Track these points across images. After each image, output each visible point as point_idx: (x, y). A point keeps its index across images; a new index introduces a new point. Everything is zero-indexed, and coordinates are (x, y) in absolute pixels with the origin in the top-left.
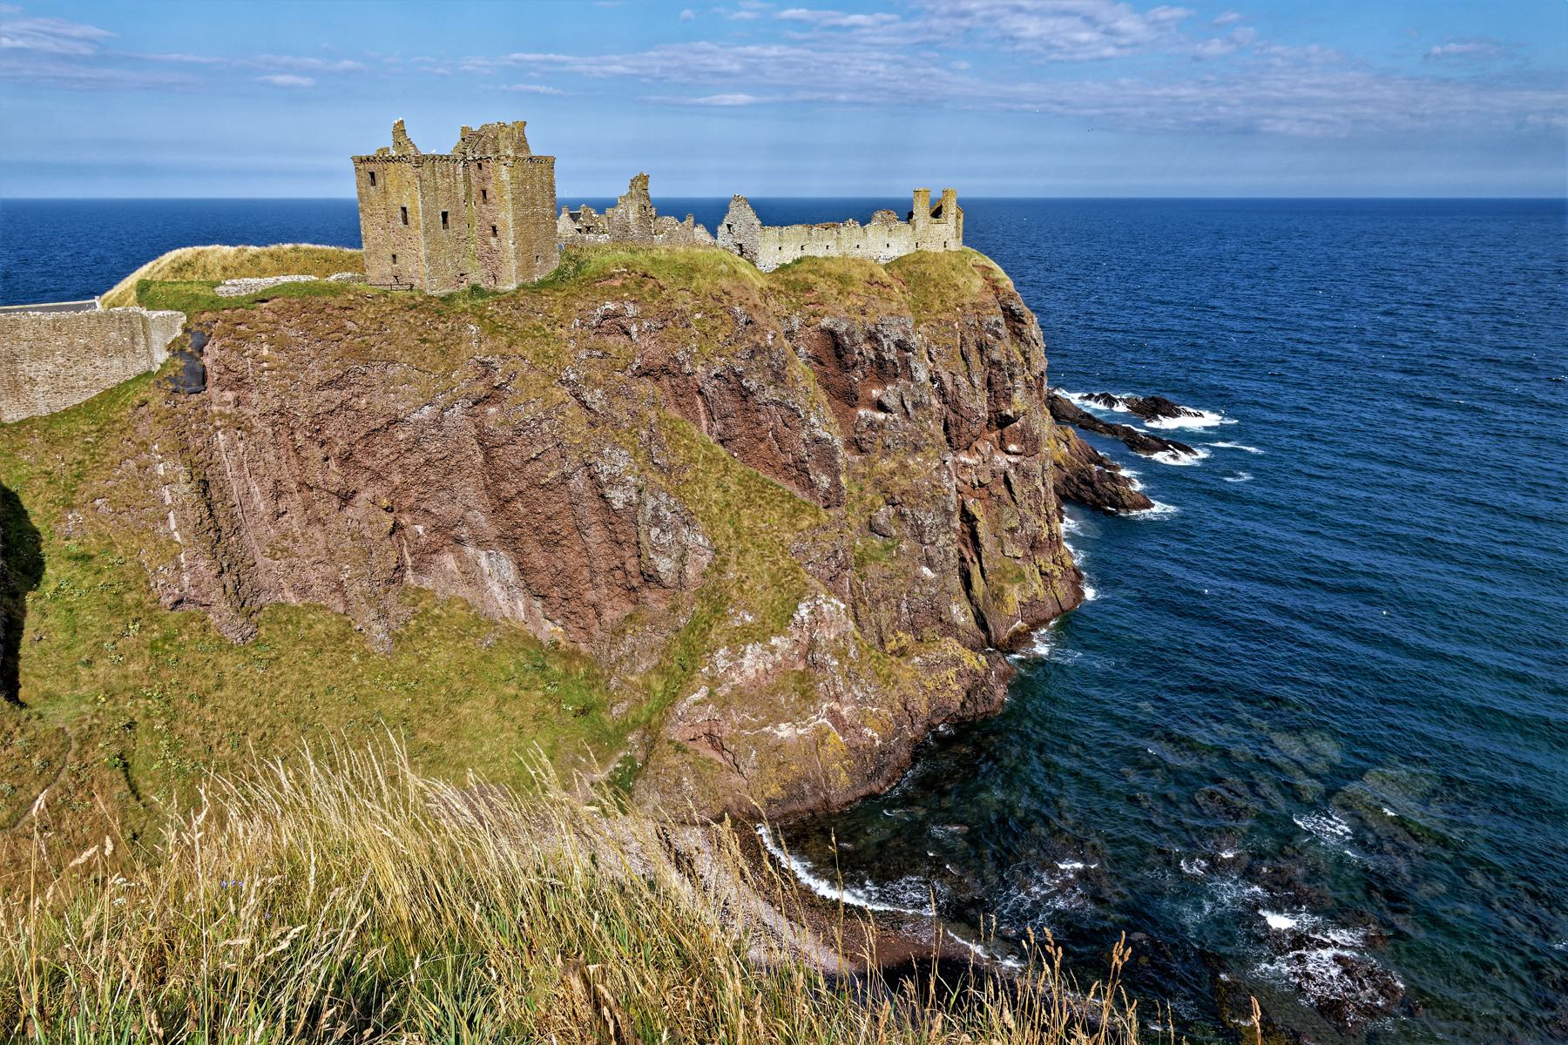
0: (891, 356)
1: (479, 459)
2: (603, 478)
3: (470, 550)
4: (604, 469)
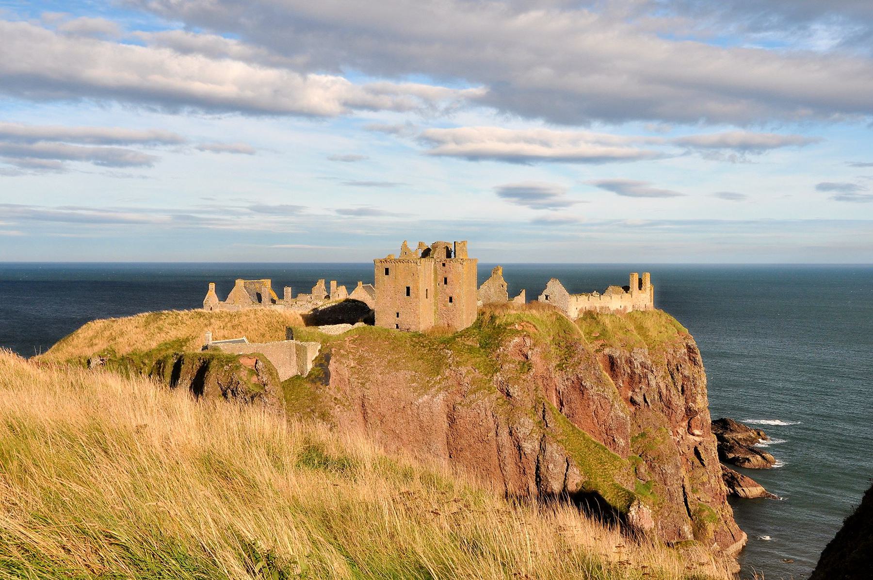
1: (446, 425)
4: (521, 432)
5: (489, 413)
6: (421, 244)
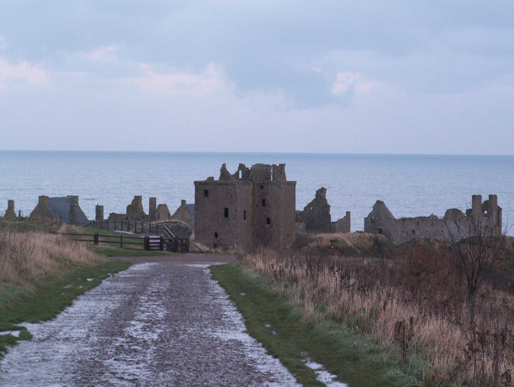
6: (242, 167)
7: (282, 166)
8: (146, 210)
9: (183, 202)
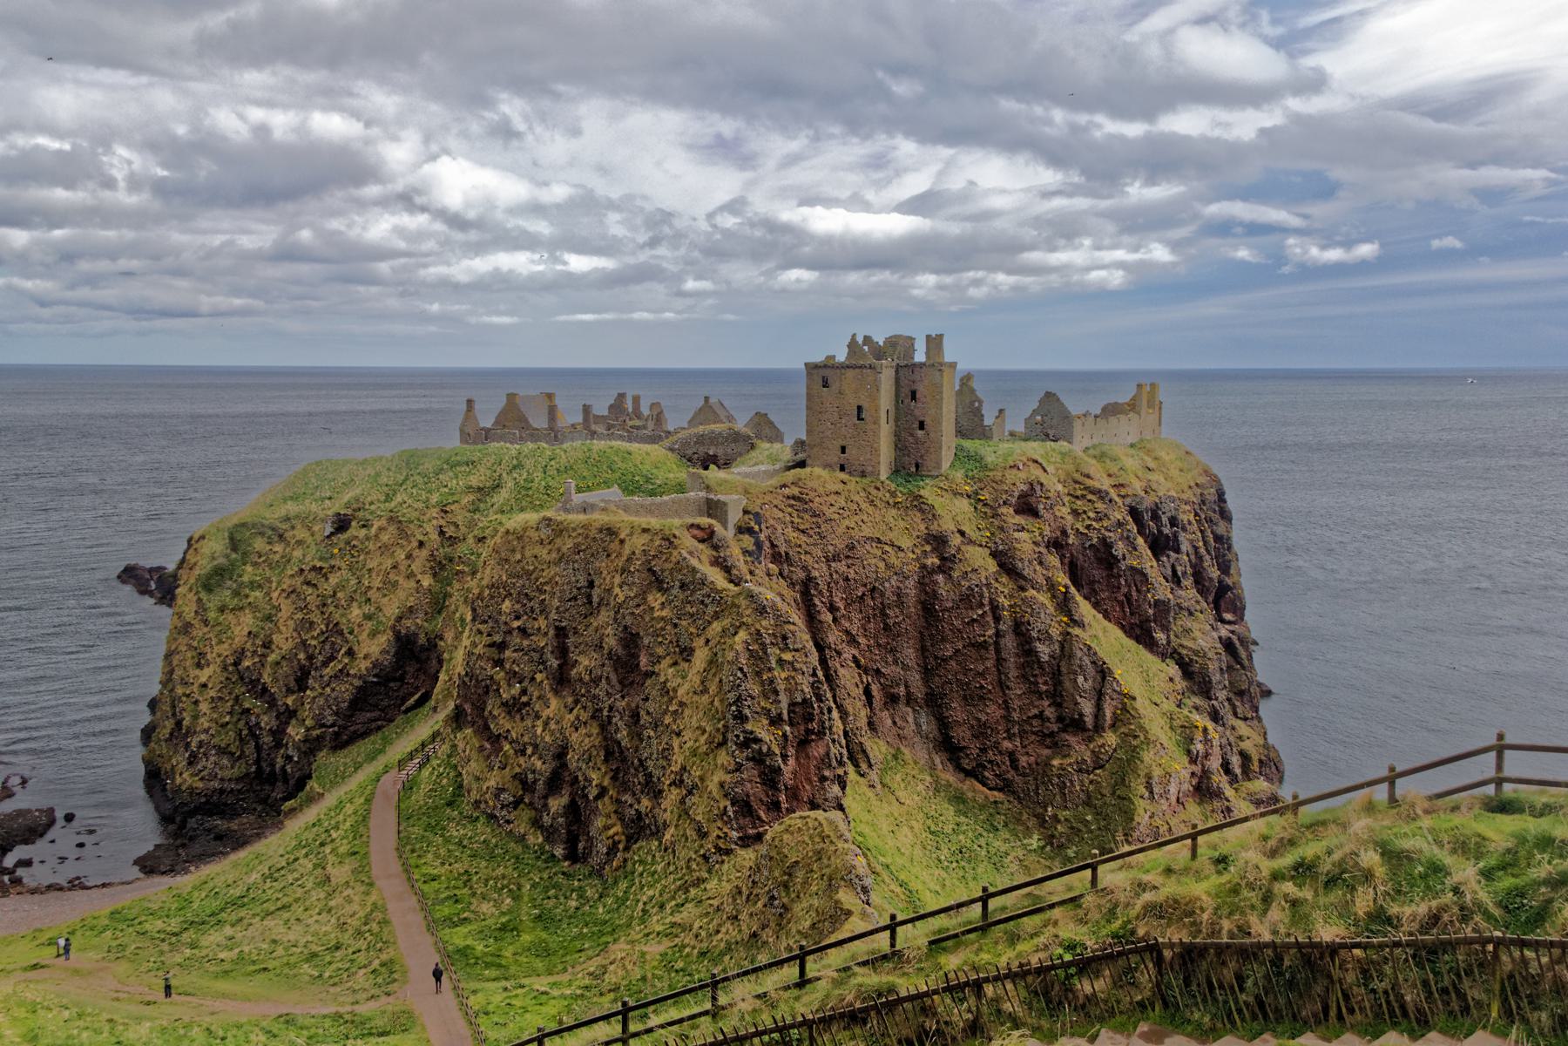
0: (1166, 531)
2: (1034, 634)
3: (903, 708)
5: (986, 601)
7: (941, 336)
8: (629, 406)
9: (707, 399)
